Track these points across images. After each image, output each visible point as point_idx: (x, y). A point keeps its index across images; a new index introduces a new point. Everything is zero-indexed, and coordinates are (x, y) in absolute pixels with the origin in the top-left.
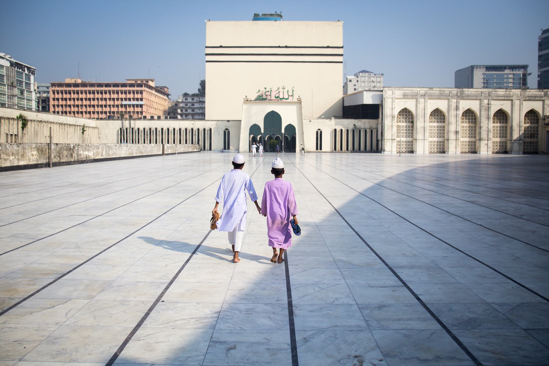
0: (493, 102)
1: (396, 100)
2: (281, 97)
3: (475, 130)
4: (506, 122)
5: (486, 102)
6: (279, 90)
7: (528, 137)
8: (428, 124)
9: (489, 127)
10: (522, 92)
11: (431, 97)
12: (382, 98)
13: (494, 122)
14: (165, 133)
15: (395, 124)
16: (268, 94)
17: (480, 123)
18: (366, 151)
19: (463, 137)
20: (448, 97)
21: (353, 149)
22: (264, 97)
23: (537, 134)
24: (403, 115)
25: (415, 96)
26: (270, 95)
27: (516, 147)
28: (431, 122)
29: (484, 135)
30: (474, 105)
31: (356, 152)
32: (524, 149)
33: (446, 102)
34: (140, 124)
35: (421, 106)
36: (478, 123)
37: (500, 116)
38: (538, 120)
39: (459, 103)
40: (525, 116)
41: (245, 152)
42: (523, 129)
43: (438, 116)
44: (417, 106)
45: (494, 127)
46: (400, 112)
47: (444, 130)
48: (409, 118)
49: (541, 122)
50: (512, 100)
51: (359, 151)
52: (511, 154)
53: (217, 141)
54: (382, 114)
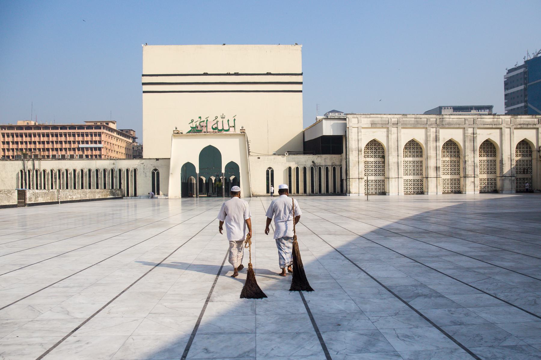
0: (478, 131)
1: (363, 130)
2: (220, 128)
3: (459, 166)
4: (495, 156)
5: (470, 131)
6: (218, 119)
7: (520, 173)
8: (402, 159)
9: (474, 160)
10: (512, 119)
11: (405, 126)
12: (345, 128)
13: (480, 156)
14: (86, 175)
15: (362, 159)
16: (204, 124)
17: (465, 157)
18: (327, 193)
19: (444, 174)
20: (425, 126)
21: (313, 191)
22: (199, 129)
23: (531, 169)
24: (371, 149)
25: (385, 125)
26: (206, 126)
27: (507, 184)
28: (406, 156)
30: (457, 135)
31: (316, 195)
32: (517, 187)
33: (423, 131)
34: (47, 165)
35: (393, 137)
36: (462, 157)
37: (488, 148)
38: (531, 151)
39: (439, 133)
40: (517, 148)
41: (176, 199)
42: (514, 163)
43: (413, 148)
44: (388, 136)
45: (480, 161)
46: (368, 145)
47: (421, 166)
48: (379, 152)
49: (535, 155)
50: (501, 128)
51: (320, 193)
52: (502, 193)
53: (144, 184)
54: (346, 148)
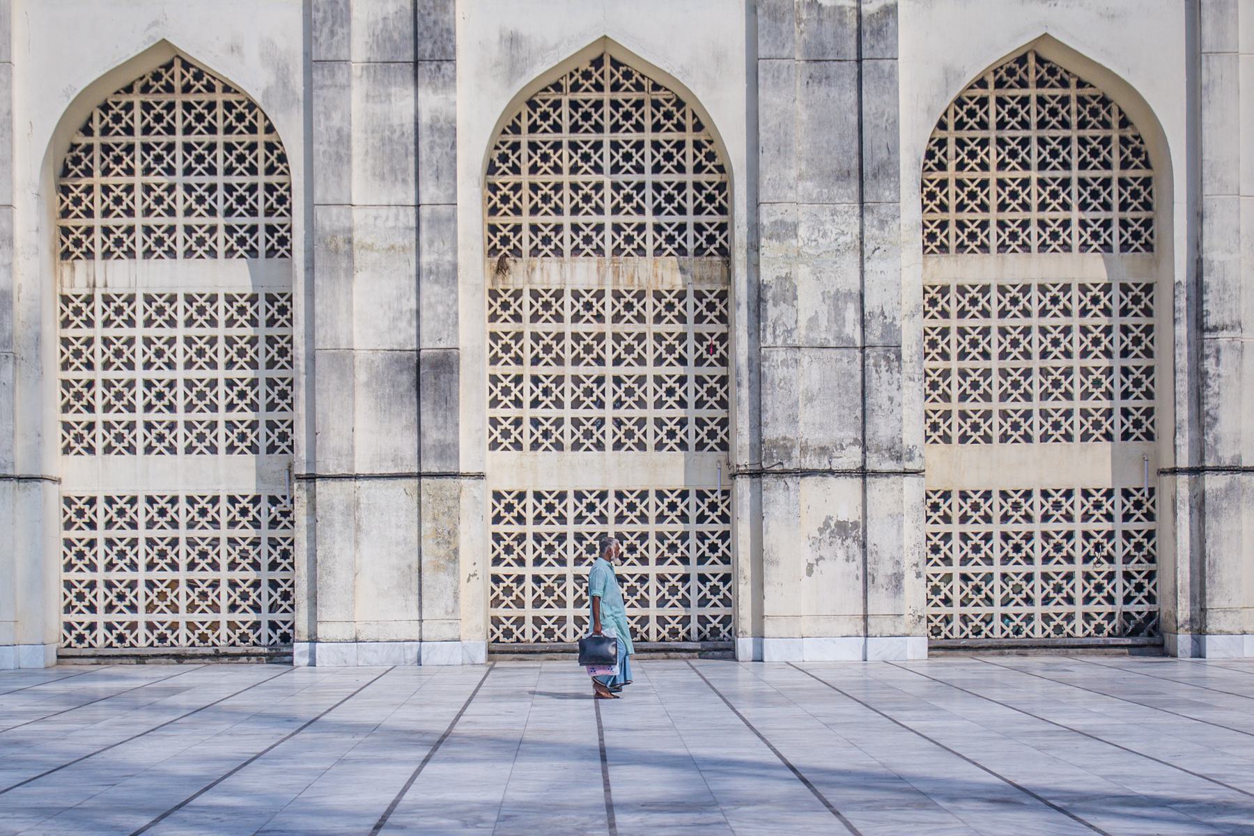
29: (804, 400)
43: (200, 159)
